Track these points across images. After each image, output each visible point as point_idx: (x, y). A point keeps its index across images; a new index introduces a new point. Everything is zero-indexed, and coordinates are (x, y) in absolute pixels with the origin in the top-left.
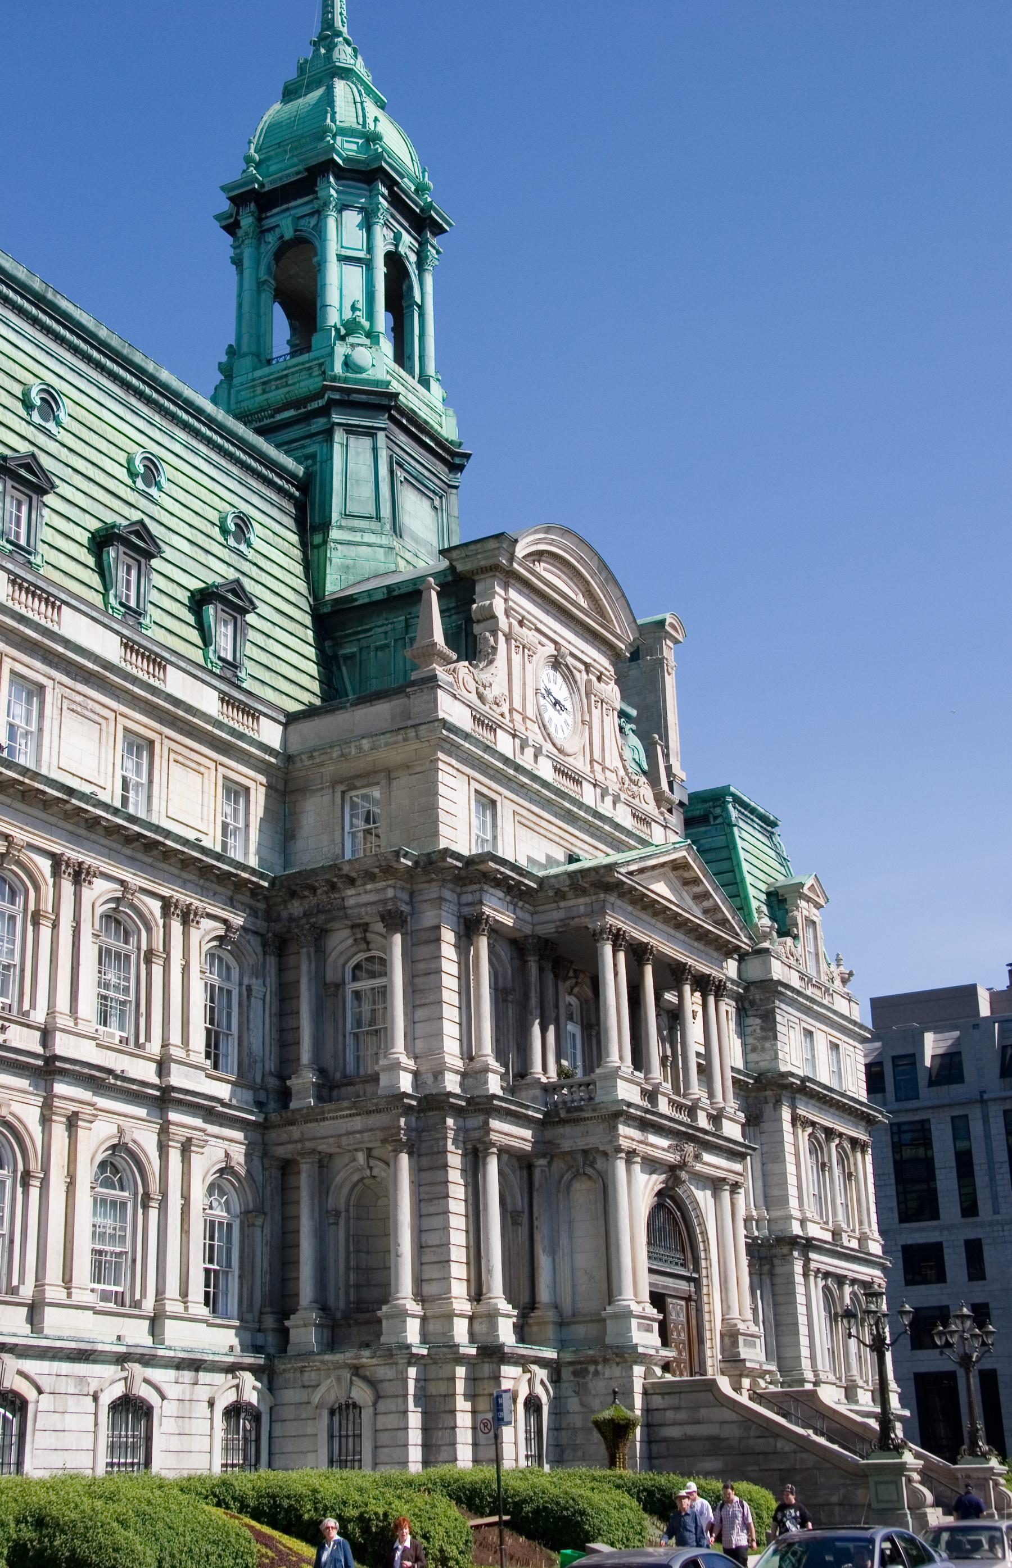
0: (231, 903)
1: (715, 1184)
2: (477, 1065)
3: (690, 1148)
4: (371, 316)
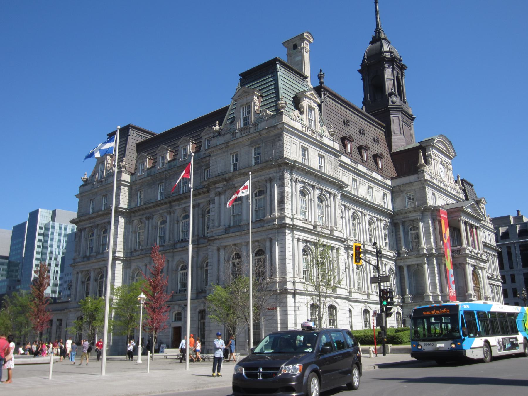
0: (386, 217)
1: (482, 268)
2: (438, 247)
3: (478, 262)
4: (395, 91)
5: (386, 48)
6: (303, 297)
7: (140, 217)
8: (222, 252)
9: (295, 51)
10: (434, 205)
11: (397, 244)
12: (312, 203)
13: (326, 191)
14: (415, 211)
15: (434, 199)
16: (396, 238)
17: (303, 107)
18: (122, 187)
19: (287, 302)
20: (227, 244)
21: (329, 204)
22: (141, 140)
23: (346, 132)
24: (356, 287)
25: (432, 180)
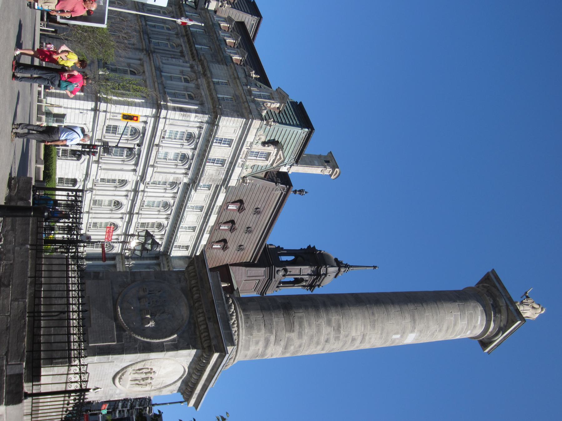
0: (165, 247)
5: (331, 270)
6: (92, 120)
7: (175, 12)
8: (139, 62)
13: (191, 164)
17: (268, 146)
19: (88, 101)
20: (145, 66)
21: (178, 167)
22: (248, 27)
23: (249, 207)
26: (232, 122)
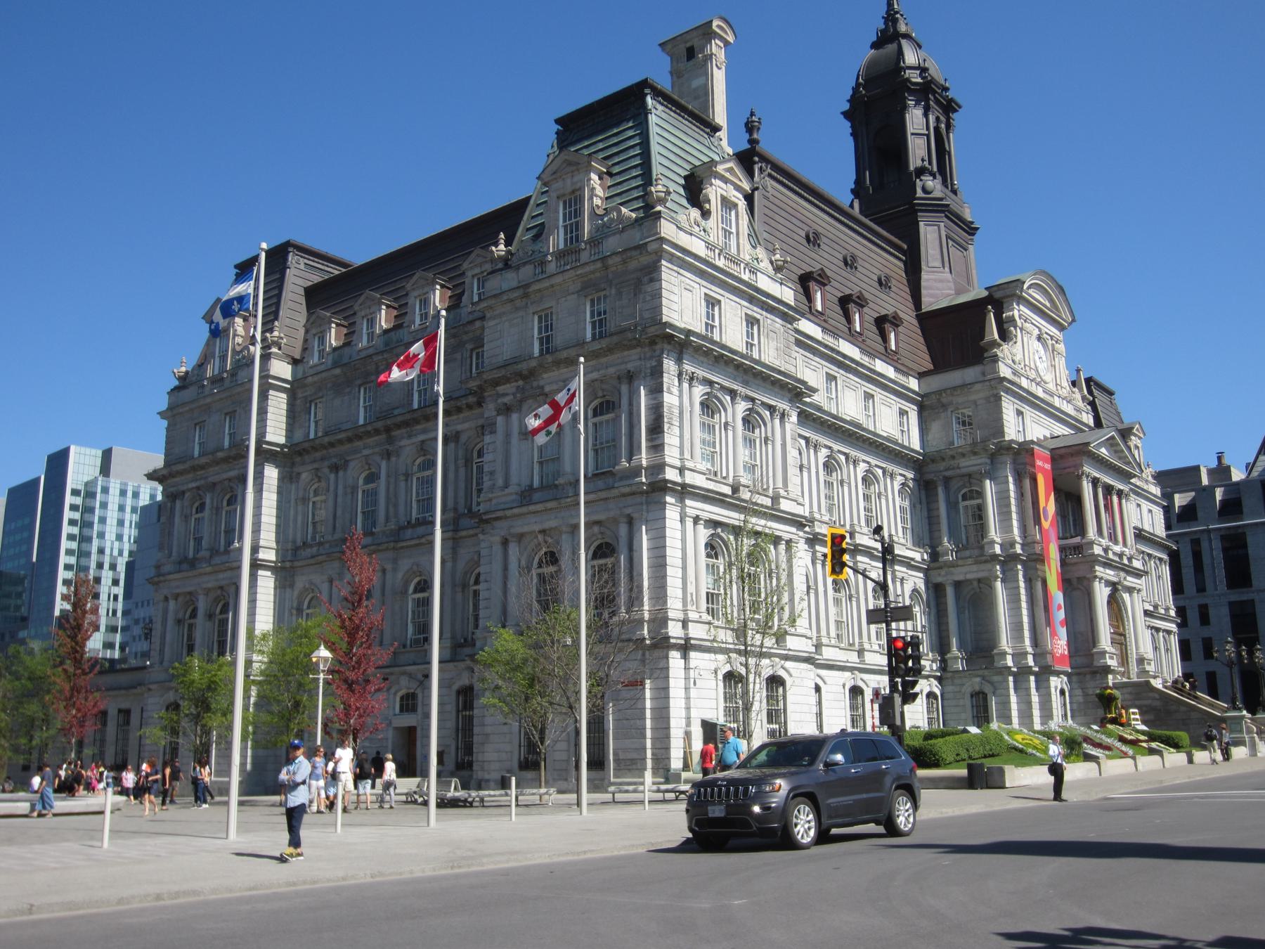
1: (1130, 590)
2: (1029, 539)
3: (1122, 574)
4: (930, 163)
5: (910, 57)
6: (706, 656)
7: (316, 465)
8: (513, 549)
9: (691, 63)
10: (1021, 440)
11: (931, 532)
12: (730, 433)
13: (763, 404)
14: (975, 453)
15: (1023, 425)
16: (929, 518)
17: (709, 201)
18: (271, 392)
19: (668, 668)
20: (526, 529)
21: (769, 434)
22: (316, 279)
23: (812, 261)
24: (833, 633)
25: (1016, 379)
26: (672, 297)
